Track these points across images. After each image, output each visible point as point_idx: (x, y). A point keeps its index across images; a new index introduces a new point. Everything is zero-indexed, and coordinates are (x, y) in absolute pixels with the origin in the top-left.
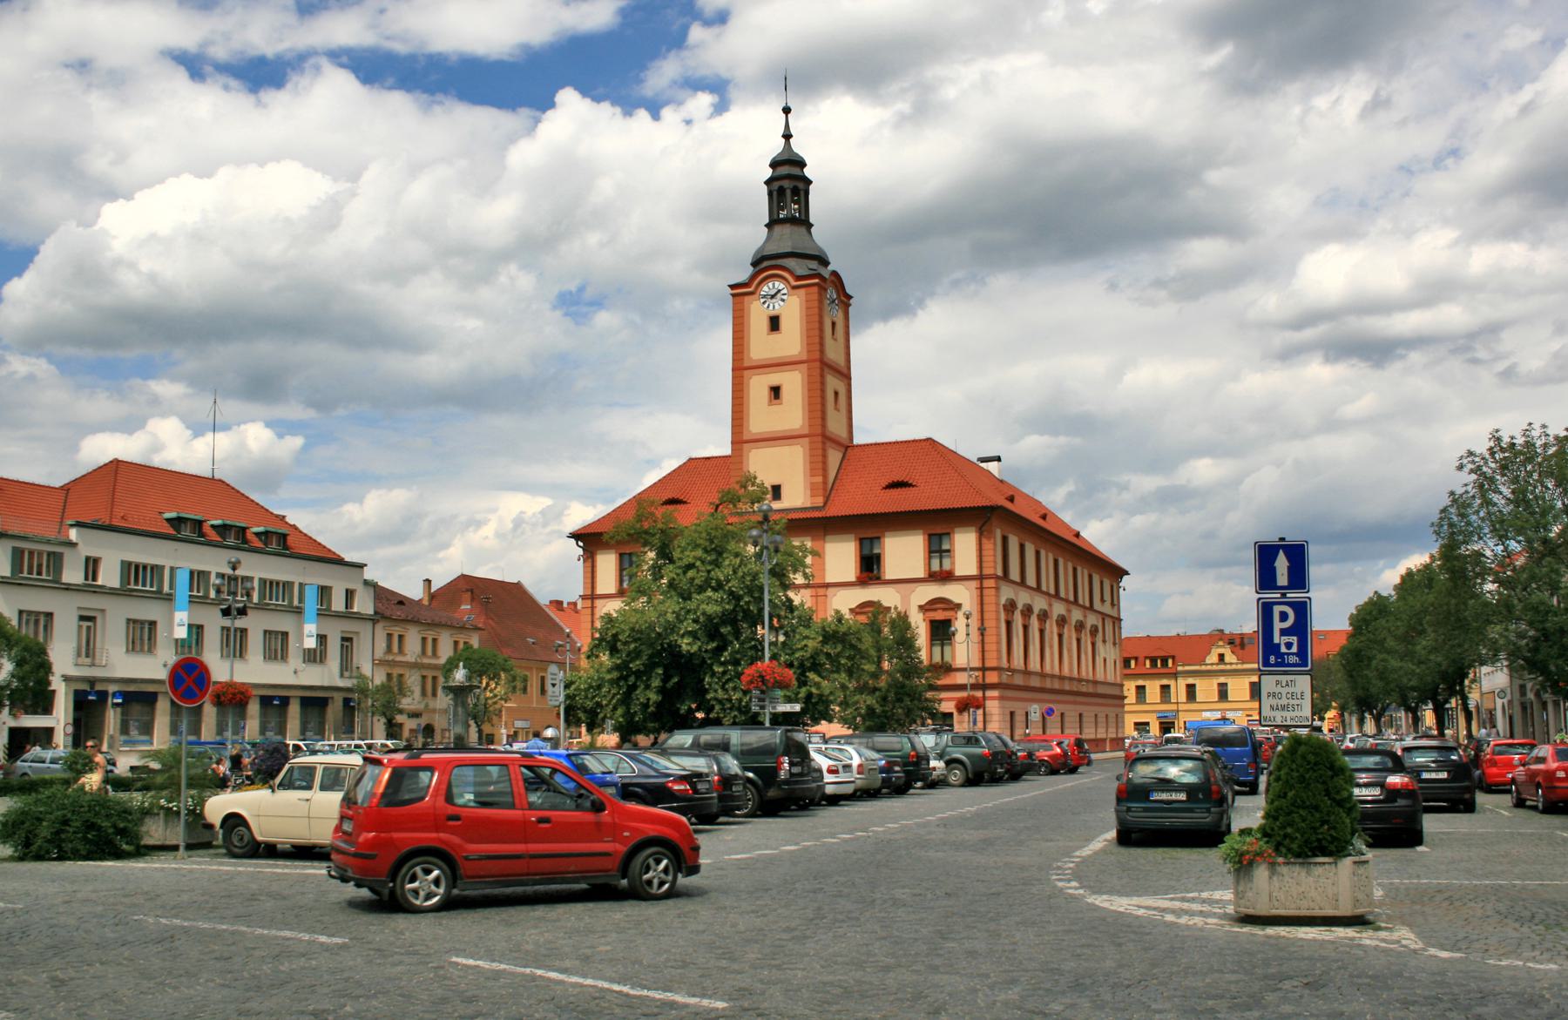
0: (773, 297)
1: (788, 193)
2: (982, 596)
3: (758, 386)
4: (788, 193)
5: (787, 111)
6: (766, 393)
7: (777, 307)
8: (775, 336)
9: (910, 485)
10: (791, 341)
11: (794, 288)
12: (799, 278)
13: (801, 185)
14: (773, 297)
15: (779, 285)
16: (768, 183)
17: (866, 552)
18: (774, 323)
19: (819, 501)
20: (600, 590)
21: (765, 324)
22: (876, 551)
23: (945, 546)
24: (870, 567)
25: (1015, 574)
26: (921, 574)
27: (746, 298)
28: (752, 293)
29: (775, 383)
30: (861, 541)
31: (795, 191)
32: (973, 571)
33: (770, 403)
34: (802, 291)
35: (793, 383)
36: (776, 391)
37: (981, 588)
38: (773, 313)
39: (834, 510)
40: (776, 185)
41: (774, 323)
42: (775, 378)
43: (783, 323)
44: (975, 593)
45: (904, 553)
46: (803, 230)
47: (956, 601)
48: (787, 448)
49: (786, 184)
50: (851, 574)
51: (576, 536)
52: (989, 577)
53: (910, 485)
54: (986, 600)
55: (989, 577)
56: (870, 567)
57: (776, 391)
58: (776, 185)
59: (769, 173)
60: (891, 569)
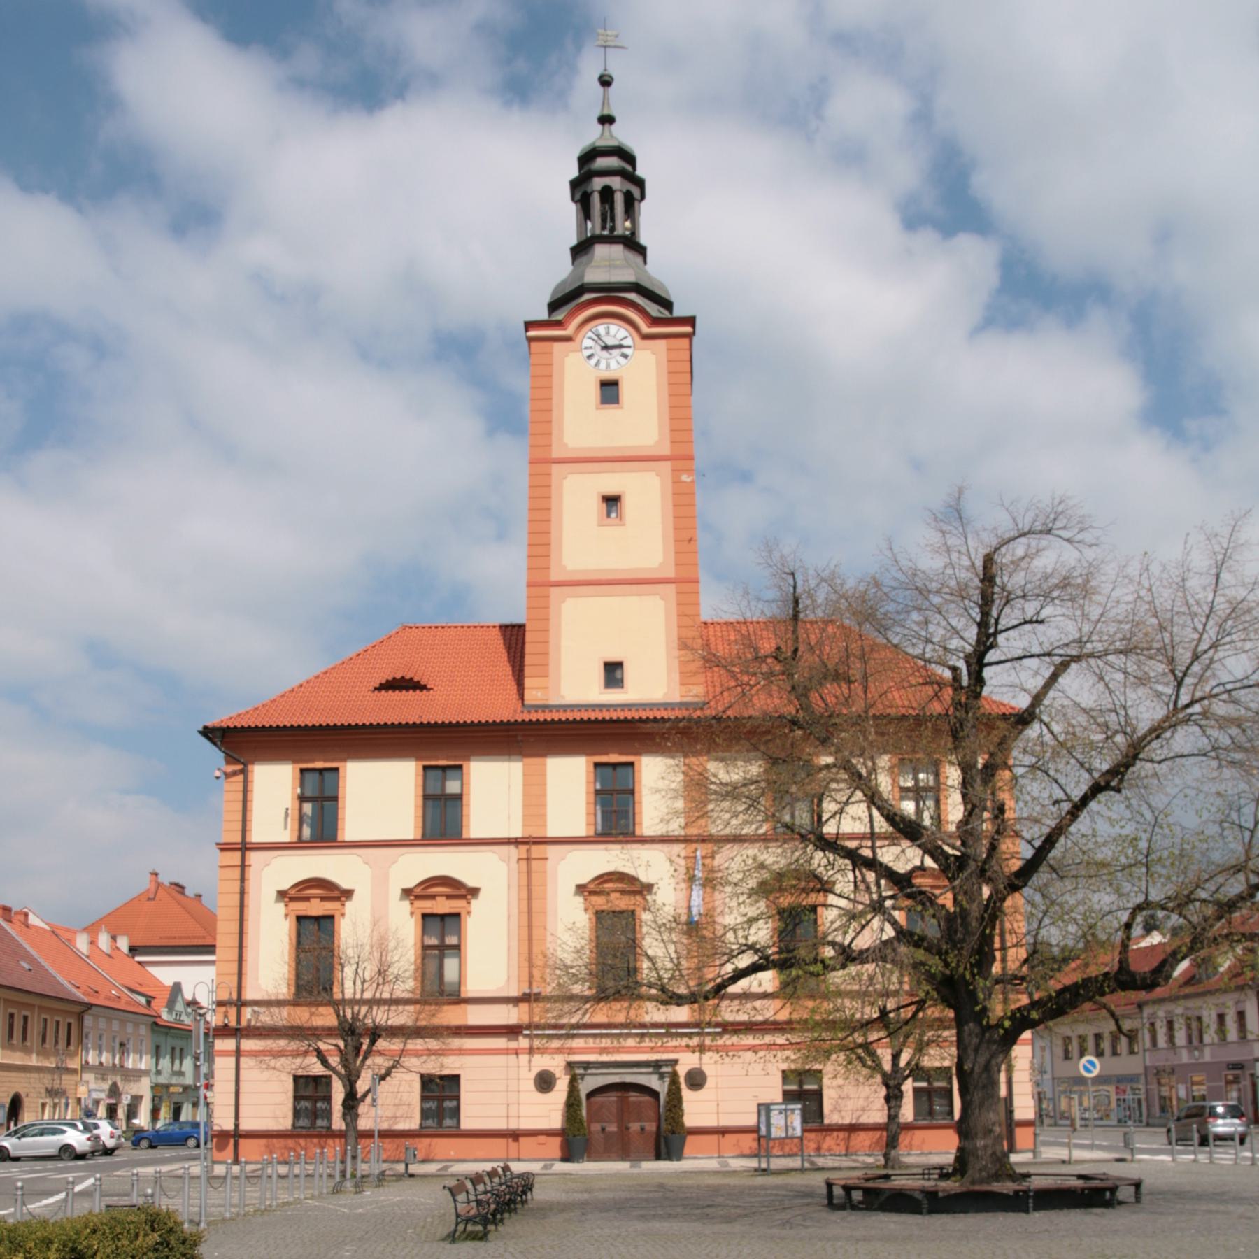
0: (606, 348)
1: (619, 199)
3: (577, 495)
4: (619, 199)
5: (605, 82)
7: (612, 366)
8: (610, 411)
10: (641, 420)
12: (656, 321)
13: (636, 192)
14: (606, 348)
15: (615, 332)
16: (575, 184)
18: (609, 389)
19: (696, 692)
20: (256, 836)
21: (594, 392)
27: (557, 346)
28: (568, 339)
29: (611, 490)
33: (600, 525)
34: (662, 344)
35: (646, 493)
41: (609, 389)
42: (611, 482)
43: (625, 390)
46: (639, 259)
48: (635, 598)
49: (616, 182)
51: (207, 733)
58: (598, 183)
59: (574, 172)
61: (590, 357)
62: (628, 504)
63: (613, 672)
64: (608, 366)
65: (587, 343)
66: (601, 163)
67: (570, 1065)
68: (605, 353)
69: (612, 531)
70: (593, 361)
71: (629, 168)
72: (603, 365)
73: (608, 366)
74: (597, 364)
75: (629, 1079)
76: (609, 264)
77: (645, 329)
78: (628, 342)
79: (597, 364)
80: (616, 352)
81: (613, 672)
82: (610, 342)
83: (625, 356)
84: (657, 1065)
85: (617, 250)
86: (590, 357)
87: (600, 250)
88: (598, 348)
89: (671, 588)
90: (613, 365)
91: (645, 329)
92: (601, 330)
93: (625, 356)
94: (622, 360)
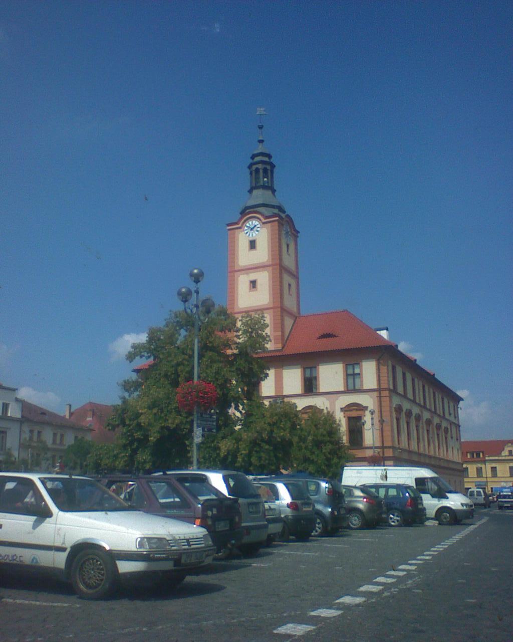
0: (252, 229)
1: (261, 171)
2: (380, 401)
4: (261, 171)
7: (254, 235)
8: (253, 252)
9: (335, 336)
10: (262, 254)
11: (264, 223)
12: (266, 217)
13: (269, 167)
15: (255, 222)
16: (250, 167)
17: (308, 375)
18: (253, 245)
21: (247, 244)
22: (314, 375)
23: (357, 371)
24: (310, 386)
25: (400, 389)
26: (342, 389)
27: (236, 230)
30: (304, 369)
31: (265, 170)
33: (250, 290)
34: (269, 225)
35: (264, 278)
36: (253, 284)
37: (380, 397)
38: (251, 239)
39: (288, 351)
40: (254, 167)
41: (253, 245)
42: (253, 276)
43: (258, 244)
44: (376, 400)
45: (331, 375)
47: (364, 404)
49: (260, 166)
52: (385, 389)
53: (335, 336)
54: (383, 404)
55: (385, 389)
56: (310, 386)
57: (253, 284)
58: (254, 167)
60: (323, 387)
61: (247, 233)
65: (246, 228)
66: (257, 159)
68: (252, 231)
71: (266, 159)
72: (251, 235)
74: (249, 235)
76: (260, 196)
77: (264, 221)
79: (249, 235)
80: (255, 229)
82: (252, 227)
83: (257, 231)
86: (247, 233)
87: (255, 192)
88: (249, 230)
89: (272, 310)
90: (254, 235)
91: (264, 221)
92: (250, 223)
94: (257, 233)
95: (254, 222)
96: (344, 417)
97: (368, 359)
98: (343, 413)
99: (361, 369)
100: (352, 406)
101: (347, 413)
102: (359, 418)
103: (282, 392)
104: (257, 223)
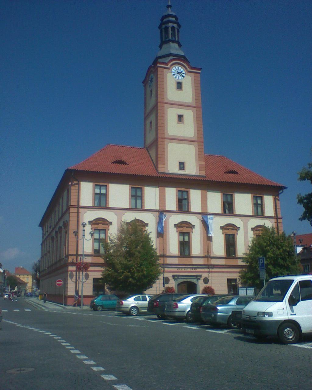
6: (176, 118)
8: (179, 92)
9: (237, 173)
10: (187, 94)
11: (189, 72)
15: (181, 69)
18: (179, 86)
19: (203, 173)
21: (174, 85)
26: (251, 213)
27: (165, 70)
28: (168, 69)
32: (272, 214)
33: (178, 123)
34: (193, 74)
35: (189, 115)
41: (179, 86)
42: (181, 111)
43: (184, 86)
50: (219, 210)
53: (237, 173)
61: (174, 75)
62: (185, 118)
63: (182, 165)
64: (179, 78)
67: (174, 276)
68: (178, 75)
69: (180, 125)
70: (175, 76)
72: (177, 78)
73: (179, 78)
74: (176, 77)
75: (189, 280)
78: (184, 72)
79: (176, 77)
81: (182, 165)
83: (183, 76)
84: (197, 276)
85: (176, 45)
86: (174, 75)
90: (180, 78)
92: (177, 67)
93: (183, 76)
95: (180, 68)
96: (177, 232)
97: (214, 190)
98: (222, 230)
99: (107, 190)
100: (184, 224)
101: (255, 232)
102: (234, 236)
103: (207, 209)
104: (182, 70)
